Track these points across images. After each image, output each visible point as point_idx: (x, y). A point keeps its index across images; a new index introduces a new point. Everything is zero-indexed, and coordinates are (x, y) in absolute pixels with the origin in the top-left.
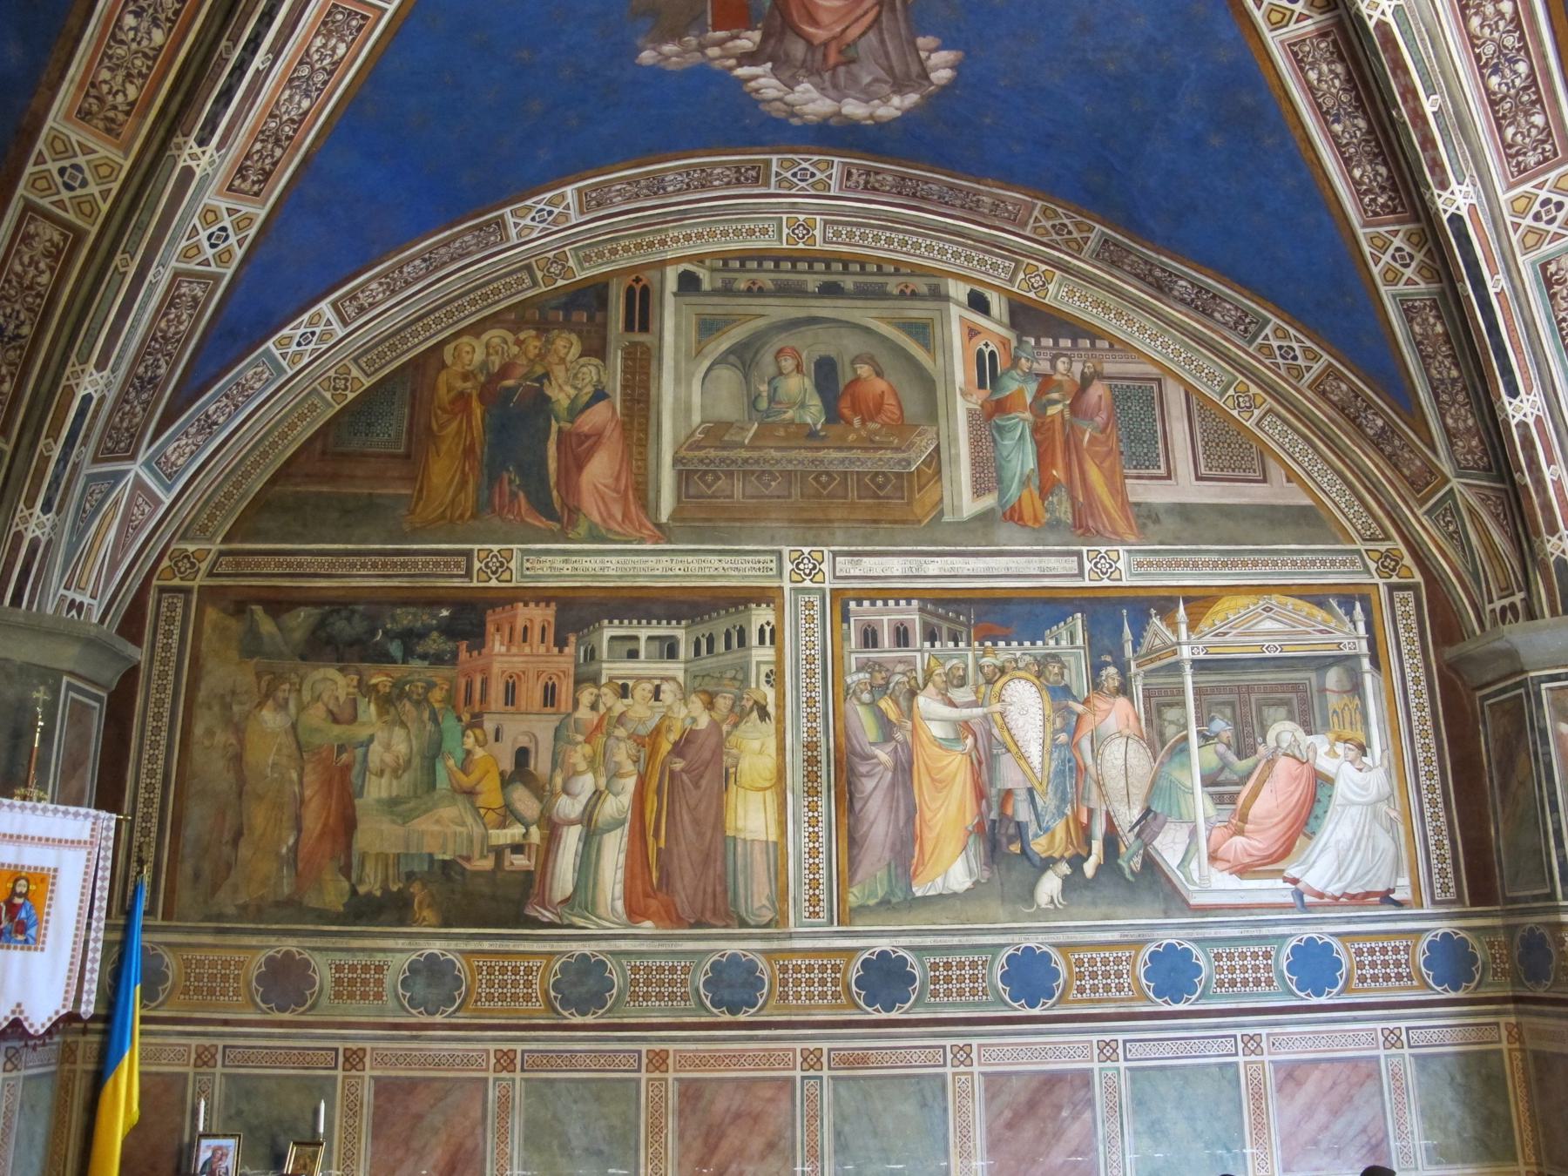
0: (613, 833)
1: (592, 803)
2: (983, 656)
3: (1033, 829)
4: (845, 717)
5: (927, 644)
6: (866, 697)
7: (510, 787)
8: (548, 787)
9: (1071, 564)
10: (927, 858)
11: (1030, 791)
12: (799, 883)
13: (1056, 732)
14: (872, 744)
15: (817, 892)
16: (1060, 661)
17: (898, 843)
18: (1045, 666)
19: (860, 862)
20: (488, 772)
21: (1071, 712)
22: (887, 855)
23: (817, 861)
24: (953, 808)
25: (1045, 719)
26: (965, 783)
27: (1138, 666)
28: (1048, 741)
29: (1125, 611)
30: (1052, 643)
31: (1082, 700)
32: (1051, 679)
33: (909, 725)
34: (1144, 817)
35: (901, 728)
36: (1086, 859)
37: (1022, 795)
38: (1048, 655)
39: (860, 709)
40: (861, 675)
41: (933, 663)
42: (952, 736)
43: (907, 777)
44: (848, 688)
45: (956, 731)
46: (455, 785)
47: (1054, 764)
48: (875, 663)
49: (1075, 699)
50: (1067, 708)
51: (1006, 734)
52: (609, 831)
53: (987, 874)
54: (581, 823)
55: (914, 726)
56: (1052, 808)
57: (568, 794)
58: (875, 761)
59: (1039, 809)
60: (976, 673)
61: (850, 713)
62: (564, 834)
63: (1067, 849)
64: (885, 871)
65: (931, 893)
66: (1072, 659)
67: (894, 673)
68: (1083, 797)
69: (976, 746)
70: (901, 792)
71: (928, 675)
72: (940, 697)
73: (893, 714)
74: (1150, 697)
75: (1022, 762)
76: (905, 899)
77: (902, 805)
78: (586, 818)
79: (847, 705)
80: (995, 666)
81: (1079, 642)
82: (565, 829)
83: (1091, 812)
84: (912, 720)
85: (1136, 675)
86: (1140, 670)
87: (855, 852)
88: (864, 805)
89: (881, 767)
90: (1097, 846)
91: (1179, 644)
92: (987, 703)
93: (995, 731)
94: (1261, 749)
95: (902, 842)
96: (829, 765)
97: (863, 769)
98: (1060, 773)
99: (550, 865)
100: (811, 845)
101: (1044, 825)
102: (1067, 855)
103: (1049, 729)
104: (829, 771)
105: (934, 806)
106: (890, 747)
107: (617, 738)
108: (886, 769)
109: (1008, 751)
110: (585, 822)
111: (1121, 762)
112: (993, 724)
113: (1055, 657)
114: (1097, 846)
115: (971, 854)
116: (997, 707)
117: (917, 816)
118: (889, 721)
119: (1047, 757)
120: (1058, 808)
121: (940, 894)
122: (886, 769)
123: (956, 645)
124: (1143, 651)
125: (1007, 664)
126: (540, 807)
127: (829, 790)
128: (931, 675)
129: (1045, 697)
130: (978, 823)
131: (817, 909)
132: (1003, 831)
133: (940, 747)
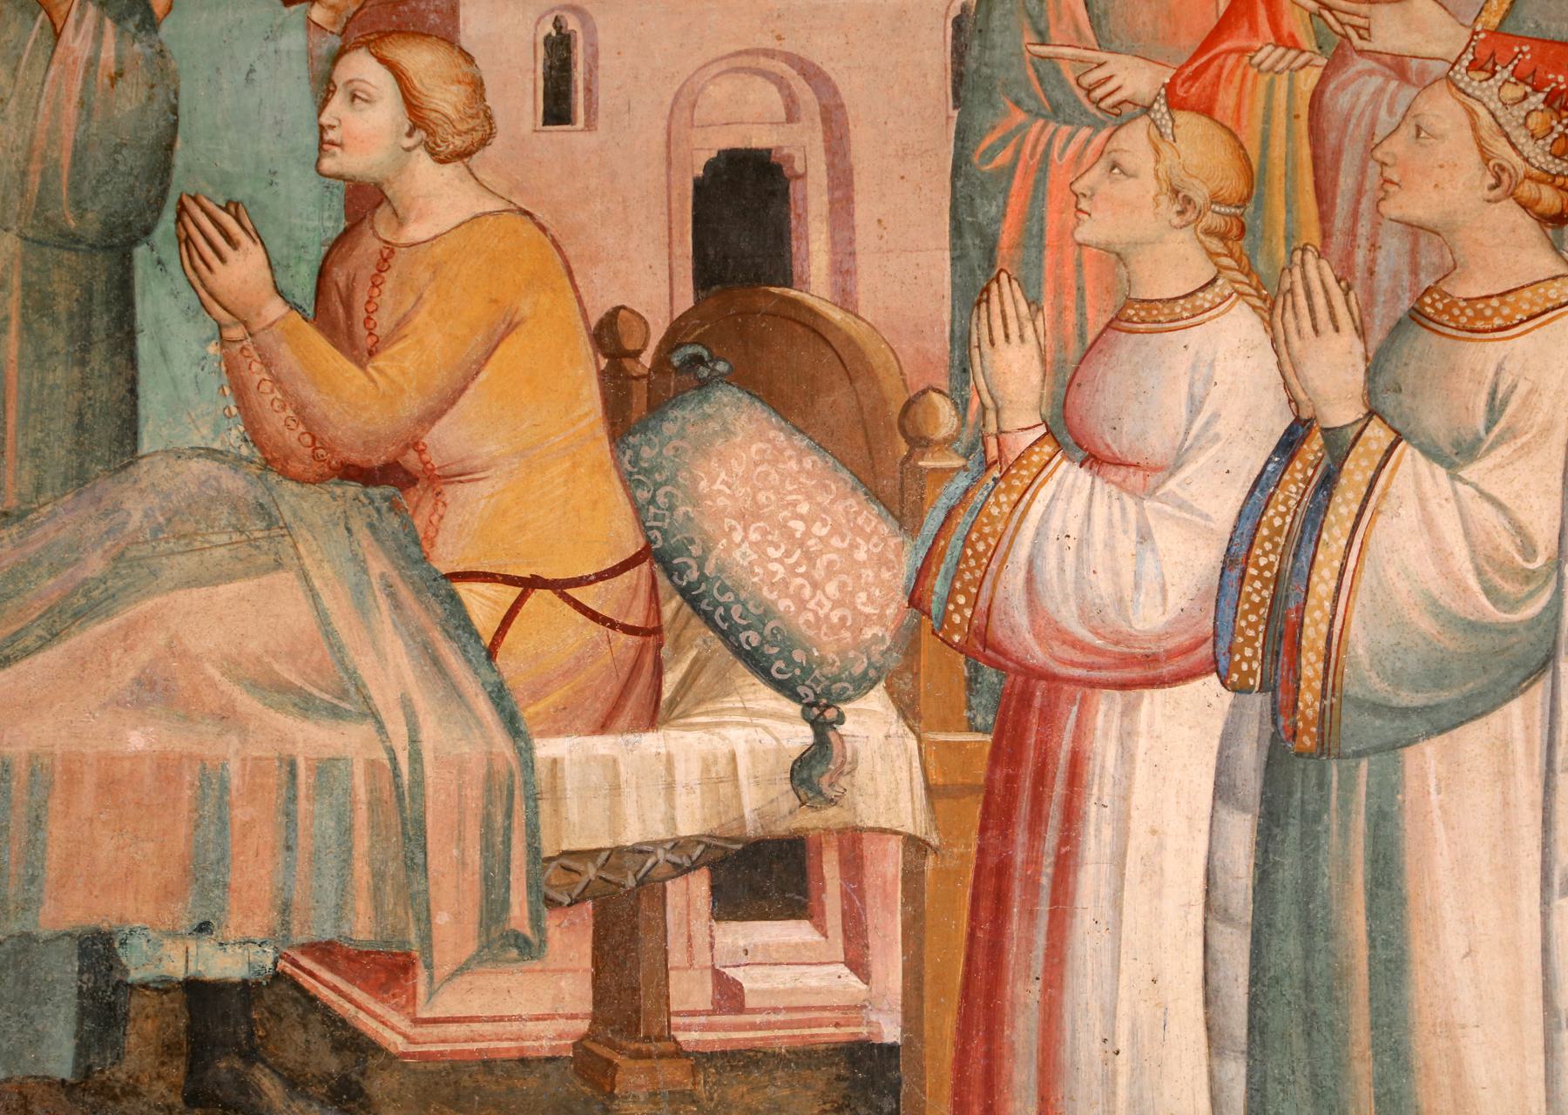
0: (1474, 738)
1: (1277, 516)
7: (680, 420)
8: (944, 417)
20: (512, 327)
46: (278, 422)
52: (1442, 720)
54: (1213, 666)
57: (1094, 460)
62: (1104, 753)
78: (1252, 625)
82: (1106, 709)
99: (1024, 994)
107: (1398, 66)
110: (1250, 659)
126: (908, 563)
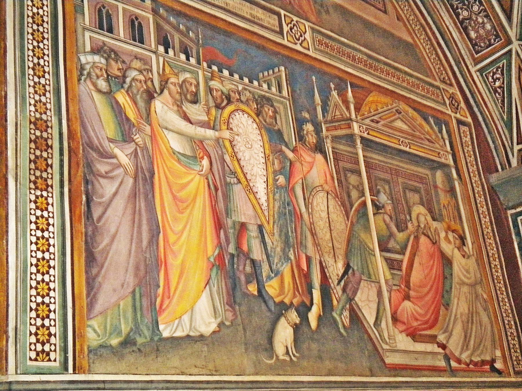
2: (212, 79)
3: (265, 269)
4: (80, 101)
5: (161, 49)
6: (102, 84)
9: (272, 21)
10: (172, 289)
11: (260, 228)
12: (22, 309)
13: (275, 173)
14: (111, 140)
15: (47, 322)
16: (272, 106)
17: (142, 268)
18: (262, 107)
19: (100, 285)
21: (286, 157)
22: (131, 280)
23: (47, 278)
24: (195, 233)
25: (266, 158)
26: (204, 206)
27: (327, 130)
28: (271, 181)
29: (314, 78)
30: (265, 86)
31: (292, 148)
32: (267, 120)
33: (148, 129)
34: (345, 273)
35: (139, 130)
36: (309, 309)
37: (253, 231)
38: (264, 97)
39: (97, 97)
40: (97, 58)
41: (168, 70)
42: (189, 153)
43: (148, 187)
44: (82, 68)
45: (193, 150)
47: (277, 205)
48: (112, 50)
49: (287, 146)
50: (281, 151)
51: (236, 163)
53: (230, 315)
55: (152, 129)
56: (278, 249)
58: (114, 161)
59: (269, 248)
60: (206, 95)
61: (85, 98)
63: (294, 296)
64: (130, 299)
65: (179, 334)
66: (282, 108)
67: (129, 68)
68: (301, 243)
69: (211, 169)
70: (143, 205)
71: (164, 83)
72: (175, 108)
73: (131, 113)
74: (338, 160)
75: (252, 197)
76: (152, 339)
77: (144, 222)
79: (82, 87)
80: (222, 92)
81: (285, 93)
83: (309, 259)
84: (150, 125)
85: (327, 137)
86: (329, 133)
87: (94, 271)
88: (104, 213)
89: (121, 170)
90: (317, 294)
91: (351, 119)
92: (218, 127)
93: (227, 158)
94: (410, 225)
95: (146, 266)
96: (61, 154)
97: (102, 167)
98: (281, 214)
100: (40, 255)
101: (274, 267)
102: (295, 301)
103: (270, 170)
104: (62, 161)
105: (178, 228)
106: (130, 148)
108: (126, 172)
109: (239, 182)
111: (324, 215)
112: (224, 150)
113: (269, 100)
114: (317, 294)
115: (215, 289)
116: (226, 134)
117: (161, 235)
118: (128, 119)
119: (271, 196)
120: (283, 250)
121: (188, 336)
122: (126, 172)
123: (188, 59)
124: (329, 118)
125: (232, 94)
127: (62, 186)
128: (167, 82)
129: (265, 138)
130: (219, 254)
131: (47, 348)
132: (241, 268)
133: (179, 161)
